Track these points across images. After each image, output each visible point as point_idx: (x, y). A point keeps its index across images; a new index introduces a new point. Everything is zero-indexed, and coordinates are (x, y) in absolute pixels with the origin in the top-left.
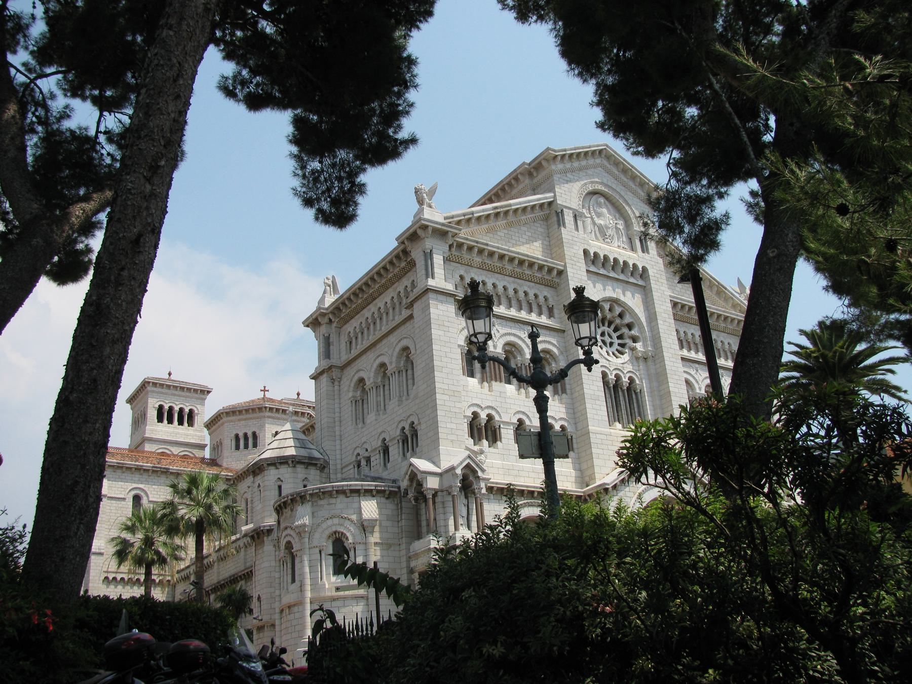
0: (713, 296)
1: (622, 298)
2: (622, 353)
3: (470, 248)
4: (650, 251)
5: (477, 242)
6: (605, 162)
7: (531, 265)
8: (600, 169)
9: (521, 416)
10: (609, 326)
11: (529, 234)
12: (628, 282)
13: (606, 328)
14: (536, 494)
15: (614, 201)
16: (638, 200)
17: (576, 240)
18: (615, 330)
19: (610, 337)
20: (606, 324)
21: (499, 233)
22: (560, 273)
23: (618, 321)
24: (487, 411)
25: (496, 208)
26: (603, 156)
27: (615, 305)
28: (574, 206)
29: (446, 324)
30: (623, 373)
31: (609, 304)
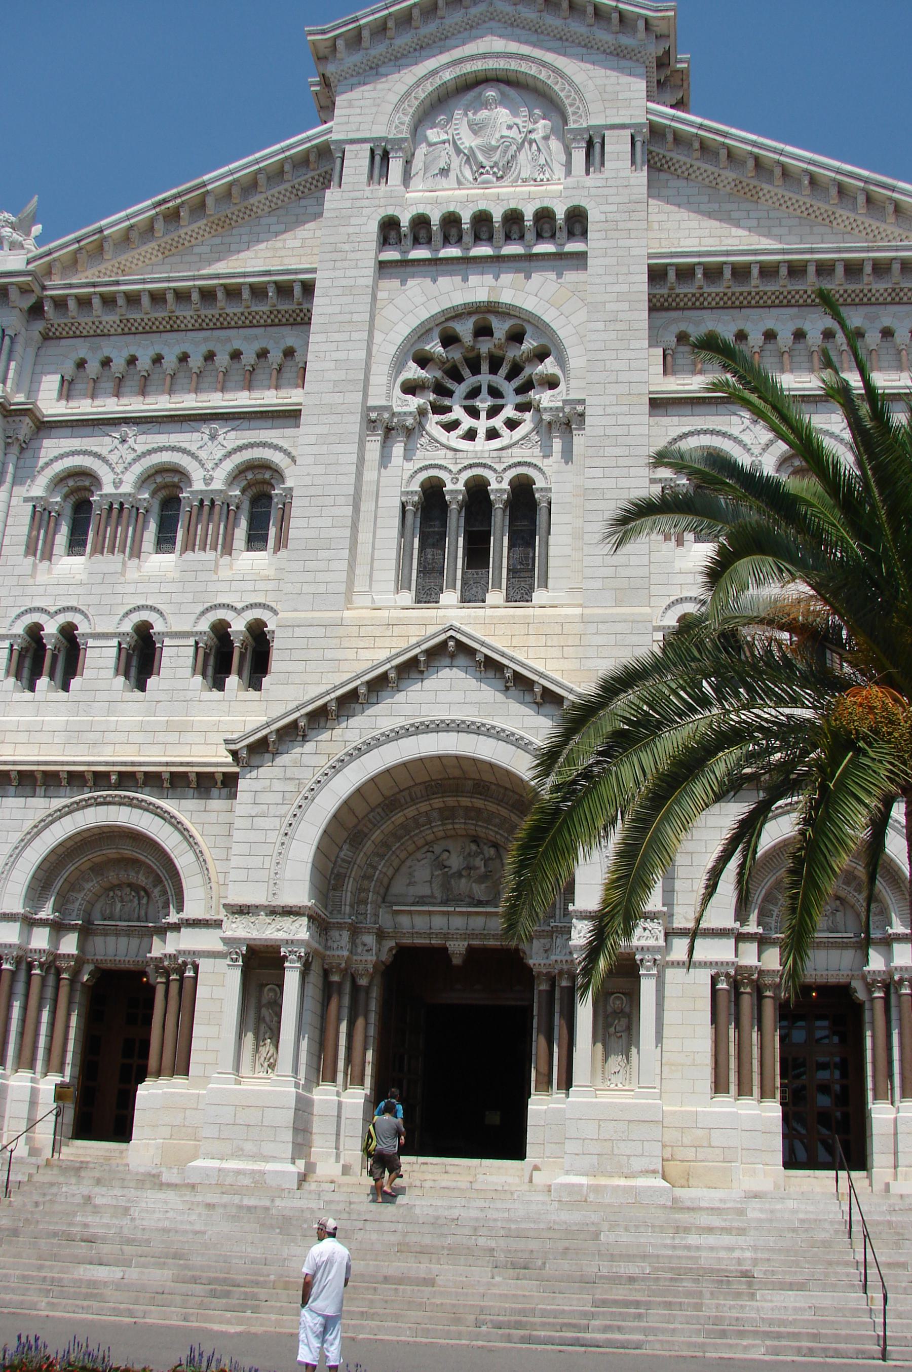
0: (860, 219)
2: (512, 424)
3: (84, 302)
5: (94, 285)
7: (232, 293)
9: (144, 616)
10: (494, 370)
12: (530, 257)
13: (485, 378)
14: (114, 778)
15: (530, 81)
17: (365, 203)
18: (509, 378)
19: (495, 392)
20: (485, 367)
21: (197, 250)
22: (308, 288)
23: (513, 353)
24: (62, 619)
25: (159, 204)
28: (379, 131)
30: (495, 470)
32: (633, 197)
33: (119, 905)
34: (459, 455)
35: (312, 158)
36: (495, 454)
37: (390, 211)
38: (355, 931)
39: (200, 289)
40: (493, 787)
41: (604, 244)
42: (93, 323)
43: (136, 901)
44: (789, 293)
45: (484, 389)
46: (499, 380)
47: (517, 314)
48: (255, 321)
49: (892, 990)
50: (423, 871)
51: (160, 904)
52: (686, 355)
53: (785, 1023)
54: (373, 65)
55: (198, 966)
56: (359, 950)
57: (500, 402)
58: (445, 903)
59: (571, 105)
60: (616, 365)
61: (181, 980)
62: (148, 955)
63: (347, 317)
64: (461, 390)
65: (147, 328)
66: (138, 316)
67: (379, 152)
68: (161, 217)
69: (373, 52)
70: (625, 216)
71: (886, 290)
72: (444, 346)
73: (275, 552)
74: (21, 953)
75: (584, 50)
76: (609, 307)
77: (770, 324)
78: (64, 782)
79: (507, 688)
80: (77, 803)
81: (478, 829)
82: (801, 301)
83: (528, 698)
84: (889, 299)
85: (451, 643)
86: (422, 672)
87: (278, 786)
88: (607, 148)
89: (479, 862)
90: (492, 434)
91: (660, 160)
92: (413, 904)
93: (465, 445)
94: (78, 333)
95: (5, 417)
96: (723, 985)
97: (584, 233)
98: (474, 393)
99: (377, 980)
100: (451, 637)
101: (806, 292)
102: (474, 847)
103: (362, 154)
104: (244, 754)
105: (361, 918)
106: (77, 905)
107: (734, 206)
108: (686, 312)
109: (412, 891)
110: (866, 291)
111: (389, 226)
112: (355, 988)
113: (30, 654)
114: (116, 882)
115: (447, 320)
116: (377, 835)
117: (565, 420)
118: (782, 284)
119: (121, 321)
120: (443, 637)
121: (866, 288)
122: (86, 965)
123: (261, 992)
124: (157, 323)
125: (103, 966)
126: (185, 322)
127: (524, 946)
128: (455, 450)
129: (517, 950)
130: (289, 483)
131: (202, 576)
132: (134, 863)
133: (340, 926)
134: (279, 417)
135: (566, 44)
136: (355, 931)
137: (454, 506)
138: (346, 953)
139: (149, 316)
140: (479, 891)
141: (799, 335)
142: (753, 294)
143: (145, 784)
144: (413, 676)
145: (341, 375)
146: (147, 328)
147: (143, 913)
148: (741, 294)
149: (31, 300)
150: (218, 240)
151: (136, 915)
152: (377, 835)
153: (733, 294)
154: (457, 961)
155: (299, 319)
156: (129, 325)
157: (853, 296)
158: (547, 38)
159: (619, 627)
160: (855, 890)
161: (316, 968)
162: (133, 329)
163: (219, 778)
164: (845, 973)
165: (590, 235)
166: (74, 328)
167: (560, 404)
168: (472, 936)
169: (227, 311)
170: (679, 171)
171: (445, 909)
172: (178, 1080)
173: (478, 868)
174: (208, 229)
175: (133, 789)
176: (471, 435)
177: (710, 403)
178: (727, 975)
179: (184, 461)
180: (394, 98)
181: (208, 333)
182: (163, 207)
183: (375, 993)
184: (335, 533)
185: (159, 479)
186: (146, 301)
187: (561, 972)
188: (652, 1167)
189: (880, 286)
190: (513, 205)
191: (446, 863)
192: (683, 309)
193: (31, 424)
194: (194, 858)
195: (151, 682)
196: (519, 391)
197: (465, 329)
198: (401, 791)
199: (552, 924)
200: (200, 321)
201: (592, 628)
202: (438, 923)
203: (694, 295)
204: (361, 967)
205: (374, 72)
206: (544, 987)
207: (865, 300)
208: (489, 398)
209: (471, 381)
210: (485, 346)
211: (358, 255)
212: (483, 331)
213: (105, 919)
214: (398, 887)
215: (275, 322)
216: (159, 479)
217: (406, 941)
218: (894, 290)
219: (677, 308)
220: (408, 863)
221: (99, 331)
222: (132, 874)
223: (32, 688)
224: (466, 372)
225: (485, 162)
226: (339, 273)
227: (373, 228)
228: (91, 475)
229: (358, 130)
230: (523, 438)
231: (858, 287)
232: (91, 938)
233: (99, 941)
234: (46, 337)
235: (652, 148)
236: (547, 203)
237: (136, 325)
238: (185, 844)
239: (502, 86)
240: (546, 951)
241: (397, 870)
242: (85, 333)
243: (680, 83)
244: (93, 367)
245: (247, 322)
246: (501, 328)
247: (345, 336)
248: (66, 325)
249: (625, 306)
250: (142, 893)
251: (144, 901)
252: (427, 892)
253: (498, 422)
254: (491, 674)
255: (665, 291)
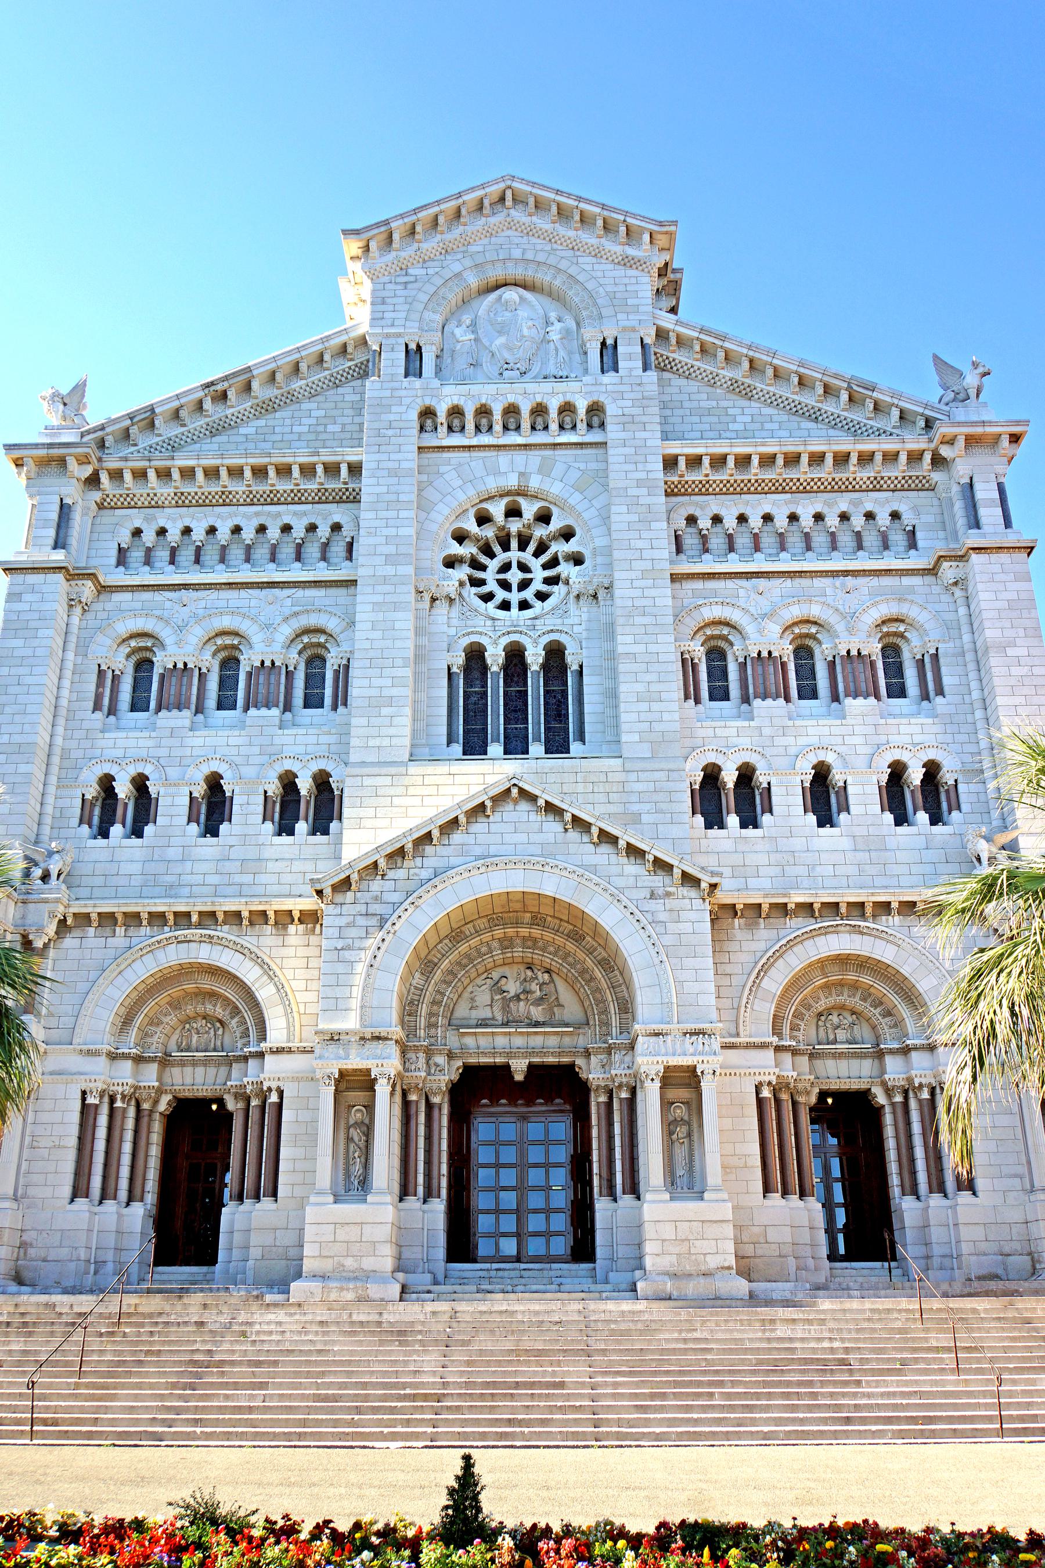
1: (534, 483)
2: (542, 596)
4: (621, 364)
6: (518, 215)
8: (509, 233)
10: (523, 547)
11: (322, 413)
13: (514, 555)
14: (195, 918)
16: (611, 266)
17: (403, 393)
18: (537, 554)
19: (523, 567)
20: (514, 544)
21: (242, 431)
22: (355, 469)
23: (540, 532)
26: (509, 202)
27: (521, 500)
29: (32, 624)
31: (505, 501)
32: (645, 394)
33: (195, 1037)
34: (497, 623)
35: (350, 350)
36: (529, 622)
37: (428, 402)
38: (429, 1053)
39: (323, 464)
40: (549, 919)
41: (623, 435)
42: (148, 495)
43: (212, 1032)
44: (784, 480)
45: (514, 565)
46: (527, 556)
47: (544, 497)
48: (303, 499)
49: (911, 1094)
50: (483, 997)
51: (238, 1035)
52: (694, 536)
53: (816, 1127)
54: (404, 267)
55: (282, 1092)
56: (433, 1071)
57: (528, 576)
58: (505, 1024)
59: (586, 309)
60: (640, 544)
61: (263, 1108)
62: (229, 1083)
63: (393, 497)
64: (493, 565)
65: (201, 501)
66: (193, 490)
67: (413, 346)
68: (209, 398)
69: (403, 254)
70: (639, 411)
71: (869, 478)
72: (479, 525)
73: (335, 708)
74: (105, 1087)
75: (594, 260)
76: (631, 492)
77: (767, 509)
78: (145, 923)
79: (566, 830)
80: (159, 942)
81: (535, 956)
82: (794, 488)
83: (586, 838)
84: (871, 486)
85: (515, 791)
86: (488, 816)
87: (361, 921)
88: (620, 349)
89: (534, 987)
90: (524, 605)
91: (664, 361)
92: (477, 1026)
93: (501, 614)
94: (132, 503)
95: (68, 580)
96: (766, 1093)
97: (602, 425)
98: (506, 568)
99: (446, 1099)
100: (515, 785)
101: (798, 480)
102: (529, 973)
103: (396, 348)
104: (328, 891)
105: (433, 1040)
106: (156, 1038)
107: (731, 404)
108: (693, 498)
109: (477, 1015)
110: (851, 479)
111: (428, 413)
112: (429, 1106)
113: (99, 803)
114: (192, 1014)
115: (481, 501)
116: (445, 965)
117: (592, 592)
118: (777, 472)
119: (175, 494)
120: (507, 785)
121: (851, 477)
122: (163, 1096)
123: (349, 1112)
124: (210, 497)
125: (181, 1095)
126: (238, 496)
127: (580, 1062)
128: (493, 619)
129: (571, 1066)
130: (345, 647)
131: (268, 731)
132: (213, 995)
133: (416, 1049)
134: (331, 586)
135: (578, 253)
136: (429, 1053)
137: (495, 668)
138: (423, 1074)
139: (202, 490)
140: (537, 1013)
141: (793, 518)
142: (753, 481)
143: (225, 923)
144: (480, 819)
145: (391, 549)
146: (201, 501)
147: (219, 1043)
148: (742, 481)
149: (88, 470)
150: (262, 423)
151: (212, 1045)
152: (445, 965)
153: (735, 481)
154: (519, 1077)
155: (344, 497)
156: (183, 498)
157: (840, 483)
158: (560, 247)
159: (657, 775)
160: (871, 1006)
161: (398, 1088)
162: (187, 502)
163: (296, 915)
164: (866, 1080)
165: (609, 427)
166: (129, 499)
167: (587, 579)
168: (532, 1054)
169: (278, 488)
170: (681, 371)
171: (507, 1030)
172: (266, 1202)
173: (534, 992)
174: (253, 411)
175: (213, 927)
176: (505, 606)
177: (719, 578)
178: (769, 1083)
179: (244, 626)
180: (424, 298)
181: (260, 508)
182: (212, 388)
183: (445, 1110)
184: (394, 692)
185: (219, 641)
186: (200, 475)
187: (620, 1086)
188: (726, 1264)
189: (865, 474)
190: (539, 400)
191: (505, 988)
192: (690, 495)
193: (93, 588)
194: (274, 990)
195: (224, 828)
196: (545, 567)
197: (497, 510)
198: (466, 924)
199: (611, 1041)
200: (251, 496)
201: (633, 776)
202: (501, 1042)
203: (701, 482)
204: (435, 1086)
205: (404, 272)
206: (603, 1099)
207: (850, 487)
208: (519, 573)
209: (502, 557)
210: (515, 526)
211: (401, 440)
212: (513, 512)
213: (182, 1051)
214: (462, 1011)
215: (322, 498)
216: (219, 641)
217: (473, 1060)
218: (875, 478)
219: (684, 495)
220: (470, 989)
221: (153, 503)
222: (209, 1007)
223: (104, 834)
224: (497, 549)
225: (510, 359)
226: (385, 457)
227: (414, 416)
228: (153, 637)
229: (393, 325)
230: (553, 609)
231: (844, 476)
232: (168, 1069)
233: (176, 1071)
234: (100, 506)
235: (657, 350)
236: (569, 398)
237: (190, 498)
238: (265, 977)
239: (520, 290)
240: (603, 1066)
241: (460, 996)
242: (140, 504)
243: (673, 292)
244: (149, 537)
245: (296, 499)
246: (529, 509)
247: (393, 514)
248: (121, 496)
249: (644, 491)
250: (218, 1025)
251: (220, 1032)
252: (490, 1015)
253: (528, 594)
254: (551, 817)
255: (676, 479)
